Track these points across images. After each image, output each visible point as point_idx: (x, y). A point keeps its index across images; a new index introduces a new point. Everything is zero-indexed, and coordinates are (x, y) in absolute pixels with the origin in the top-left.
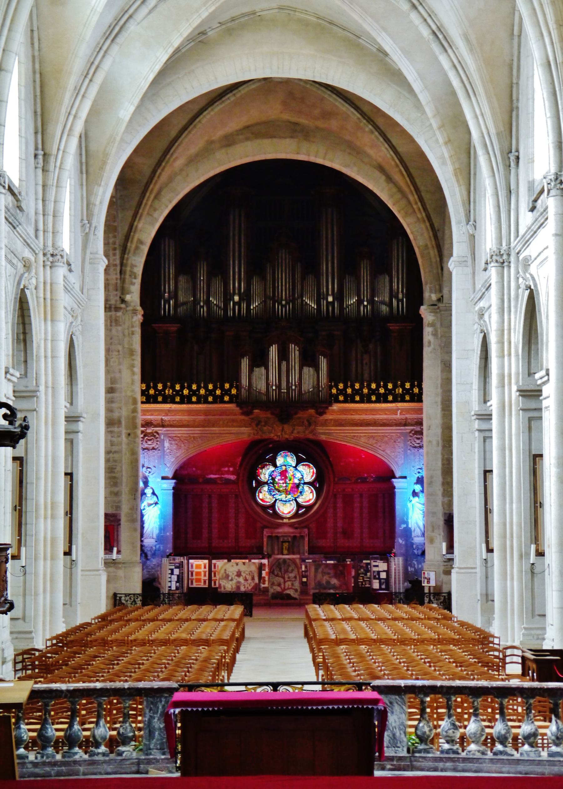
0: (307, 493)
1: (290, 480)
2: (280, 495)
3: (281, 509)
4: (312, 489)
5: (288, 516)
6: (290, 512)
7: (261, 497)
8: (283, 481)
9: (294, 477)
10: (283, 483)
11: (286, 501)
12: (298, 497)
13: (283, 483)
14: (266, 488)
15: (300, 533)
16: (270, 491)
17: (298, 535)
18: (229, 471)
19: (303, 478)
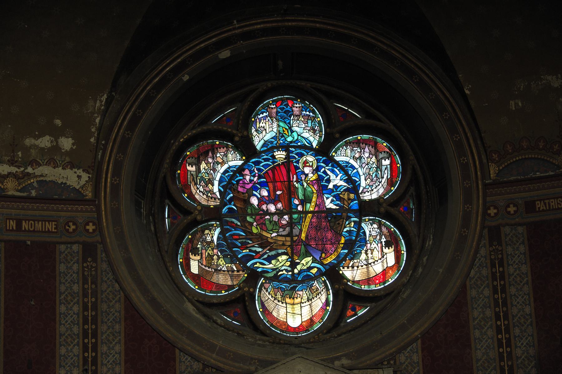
0: (374, 245)
2: (269, 260)
10: (280, 213)
16: (231, 246)
18: (56, 148)
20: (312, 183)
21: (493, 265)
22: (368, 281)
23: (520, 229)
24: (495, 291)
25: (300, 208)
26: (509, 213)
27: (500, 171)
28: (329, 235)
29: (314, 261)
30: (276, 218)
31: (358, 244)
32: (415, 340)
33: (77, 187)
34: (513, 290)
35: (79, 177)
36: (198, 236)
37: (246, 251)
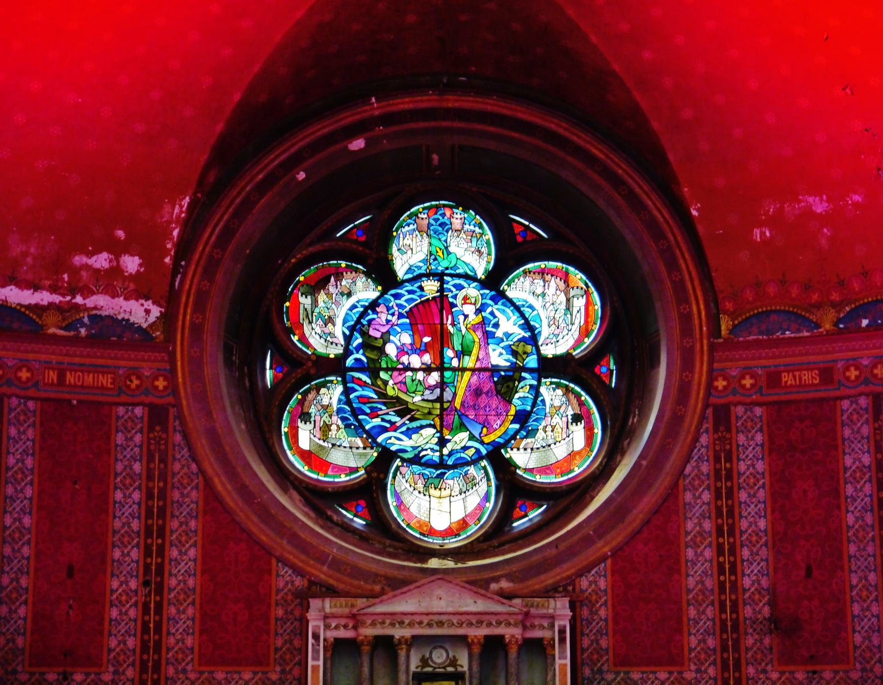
0: (556, 420)
1: (461, 354)
2: (409, 433)
3: (413, 510)
4: (585, 397)
5: (452, 543)
6: (464, 524)
7: (304, 443)
8: (427, 358)
9: (488, 336)
10: (428, 370)
11: (441, 465)
12: (505, 445)
13: (428, 370)
14: (333, 394)
15: (526, 620)
16: (355, 413)
17: (513, 633)
18: (116, 271)
19: (533, 339)
20: (474, 328)
21: (717, 459)
22: (545, 470)
23: (758, 411)
24: (718, 495)
25: (455, 363)
26: (743, 386)
27: (734, 326)
28: (495, 402)
29: (472, 437)
30: (420, 375)
31: (534, 417)
32: (603, 559)
33: (145, 326)
34: (743, 496)
35: (148, 312)
36: (310, 396)
37: (377, 421)
